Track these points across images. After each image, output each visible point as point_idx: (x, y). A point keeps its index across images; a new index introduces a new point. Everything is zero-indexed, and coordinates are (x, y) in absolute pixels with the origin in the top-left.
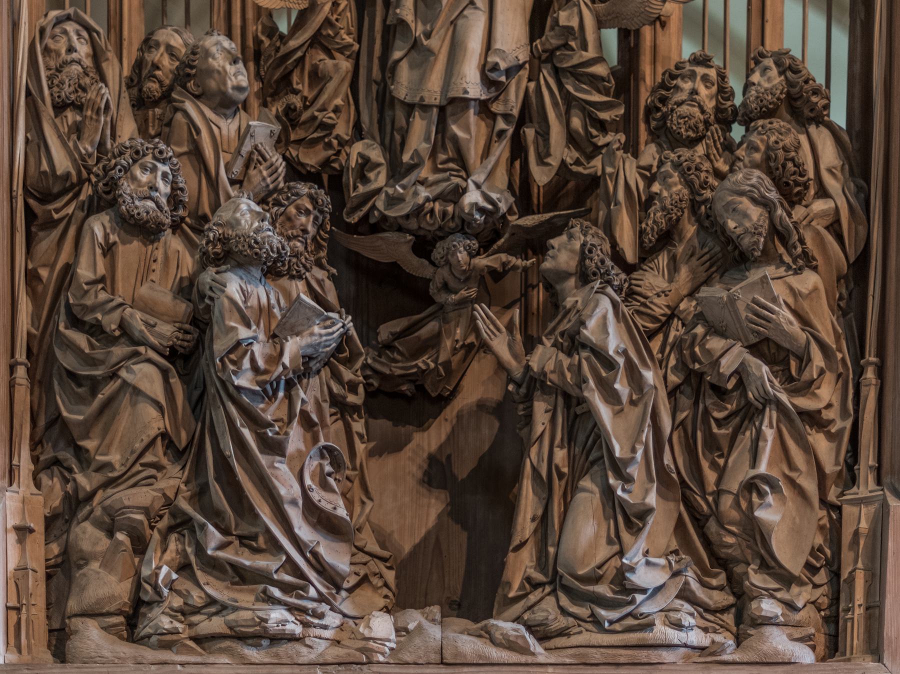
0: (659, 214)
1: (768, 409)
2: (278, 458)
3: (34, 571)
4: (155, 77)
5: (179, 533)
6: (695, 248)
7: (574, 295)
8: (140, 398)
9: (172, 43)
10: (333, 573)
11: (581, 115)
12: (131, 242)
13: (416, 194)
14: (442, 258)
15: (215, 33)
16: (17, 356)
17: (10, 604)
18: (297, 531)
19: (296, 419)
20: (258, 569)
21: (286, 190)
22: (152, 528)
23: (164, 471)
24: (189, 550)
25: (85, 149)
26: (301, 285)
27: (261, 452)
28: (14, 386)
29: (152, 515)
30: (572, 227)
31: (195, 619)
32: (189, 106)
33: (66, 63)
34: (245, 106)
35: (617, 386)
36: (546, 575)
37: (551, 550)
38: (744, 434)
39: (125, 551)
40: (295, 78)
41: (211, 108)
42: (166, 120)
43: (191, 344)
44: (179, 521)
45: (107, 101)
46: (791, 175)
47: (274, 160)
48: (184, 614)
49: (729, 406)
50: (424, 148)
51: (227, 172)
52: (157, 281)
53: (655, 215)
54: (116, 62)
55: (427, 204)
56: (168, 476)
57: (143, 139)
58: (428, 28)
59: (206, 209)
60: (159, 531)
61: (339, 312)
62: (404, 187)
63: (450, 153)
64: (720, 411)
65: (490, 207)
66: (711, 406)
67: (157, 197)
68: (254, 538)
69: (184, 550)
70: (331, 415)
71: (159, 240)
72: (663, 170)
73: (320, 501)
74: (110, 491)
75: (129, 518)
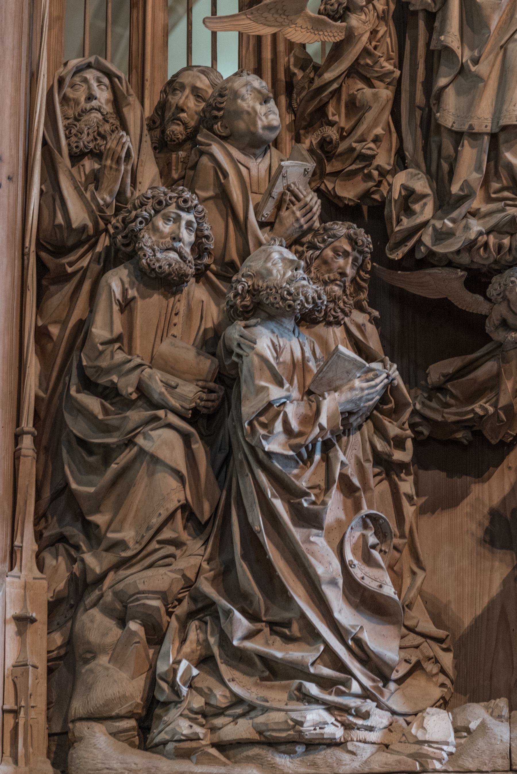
2: (315, 531)
3: (35, 667)
4: (179, 119)
5: (200, 620)
8: (159, 467)
9: (199, 84)
10: (380, 663)
12: (151, 296)
13: (467, 228)
15: (245, 73)
16: (24, 424)
17: (6, 707)
18: (336, 615)
19: (335, 486)
20: (291, 662)
21: (321, 232)
22: (170, 614)
23: (184, 548)
24: (212, 640)
25: (103, 199)
26: (339, 332)
27: (295, 525)
28: (19, 458)
29: (170, 600)
31: (218, 721)
32: (216, 150)
33: (85, 112)
34: (276, 143)
39: (139, 642)
40: (331, 109)
41: (239, 149)
42: (190, 164)
43: (216, 404)
44: (200, 605)
45: (129, 148)
47: (308, 199)
48: (205, 716)
50: (476, 178)
51: (256, 214)
52: (179, 336)
54: (137, 104)
55: (480, 238)
56: (188, 553)
57: (167, 187)
58: (476, 53)
59: (233, 254)
60: (178, 618)
61: (382, 361)
62: (453, 221)
63: (504, 181)
67: (181, 247)
68: (288, 624)
69: (206, 640)
70: (374, 476)
71: (182, 291)
73: (363, 578)
74: (122, 573)
75: (144, 604)
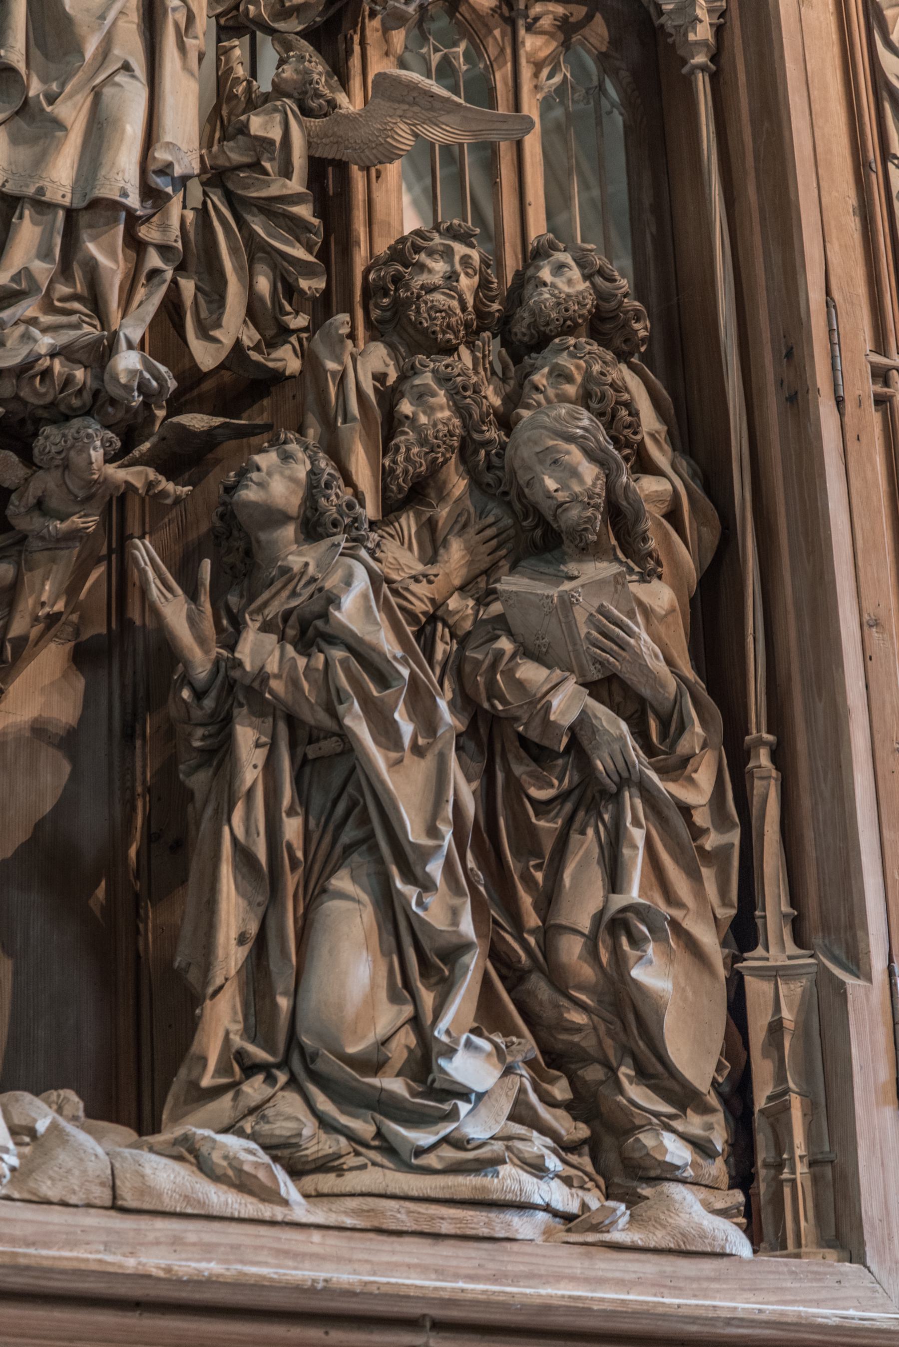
0: (415, 450)
1: (627, 794)
6: (469, 514)
7: (300, 554)
11: (271, 277)
14: (59, 453)
30: (285, 443)
35: (397, 716)
36: (271, 1050)
37: (284, 1003)
38: (583, 832)
46: (626, 427)
49: (556, 782)
53: (408, 450)
64: (540, 788)
65: (154, 383)
66: (524, 777)
72: (417, 382)
